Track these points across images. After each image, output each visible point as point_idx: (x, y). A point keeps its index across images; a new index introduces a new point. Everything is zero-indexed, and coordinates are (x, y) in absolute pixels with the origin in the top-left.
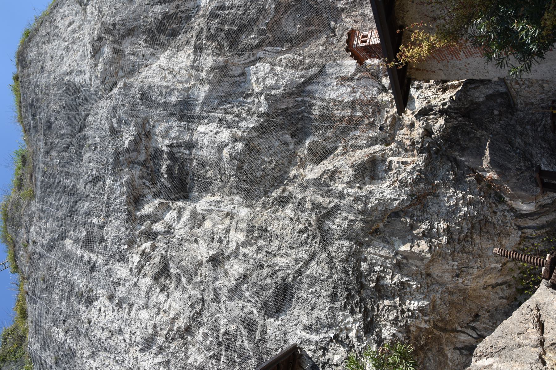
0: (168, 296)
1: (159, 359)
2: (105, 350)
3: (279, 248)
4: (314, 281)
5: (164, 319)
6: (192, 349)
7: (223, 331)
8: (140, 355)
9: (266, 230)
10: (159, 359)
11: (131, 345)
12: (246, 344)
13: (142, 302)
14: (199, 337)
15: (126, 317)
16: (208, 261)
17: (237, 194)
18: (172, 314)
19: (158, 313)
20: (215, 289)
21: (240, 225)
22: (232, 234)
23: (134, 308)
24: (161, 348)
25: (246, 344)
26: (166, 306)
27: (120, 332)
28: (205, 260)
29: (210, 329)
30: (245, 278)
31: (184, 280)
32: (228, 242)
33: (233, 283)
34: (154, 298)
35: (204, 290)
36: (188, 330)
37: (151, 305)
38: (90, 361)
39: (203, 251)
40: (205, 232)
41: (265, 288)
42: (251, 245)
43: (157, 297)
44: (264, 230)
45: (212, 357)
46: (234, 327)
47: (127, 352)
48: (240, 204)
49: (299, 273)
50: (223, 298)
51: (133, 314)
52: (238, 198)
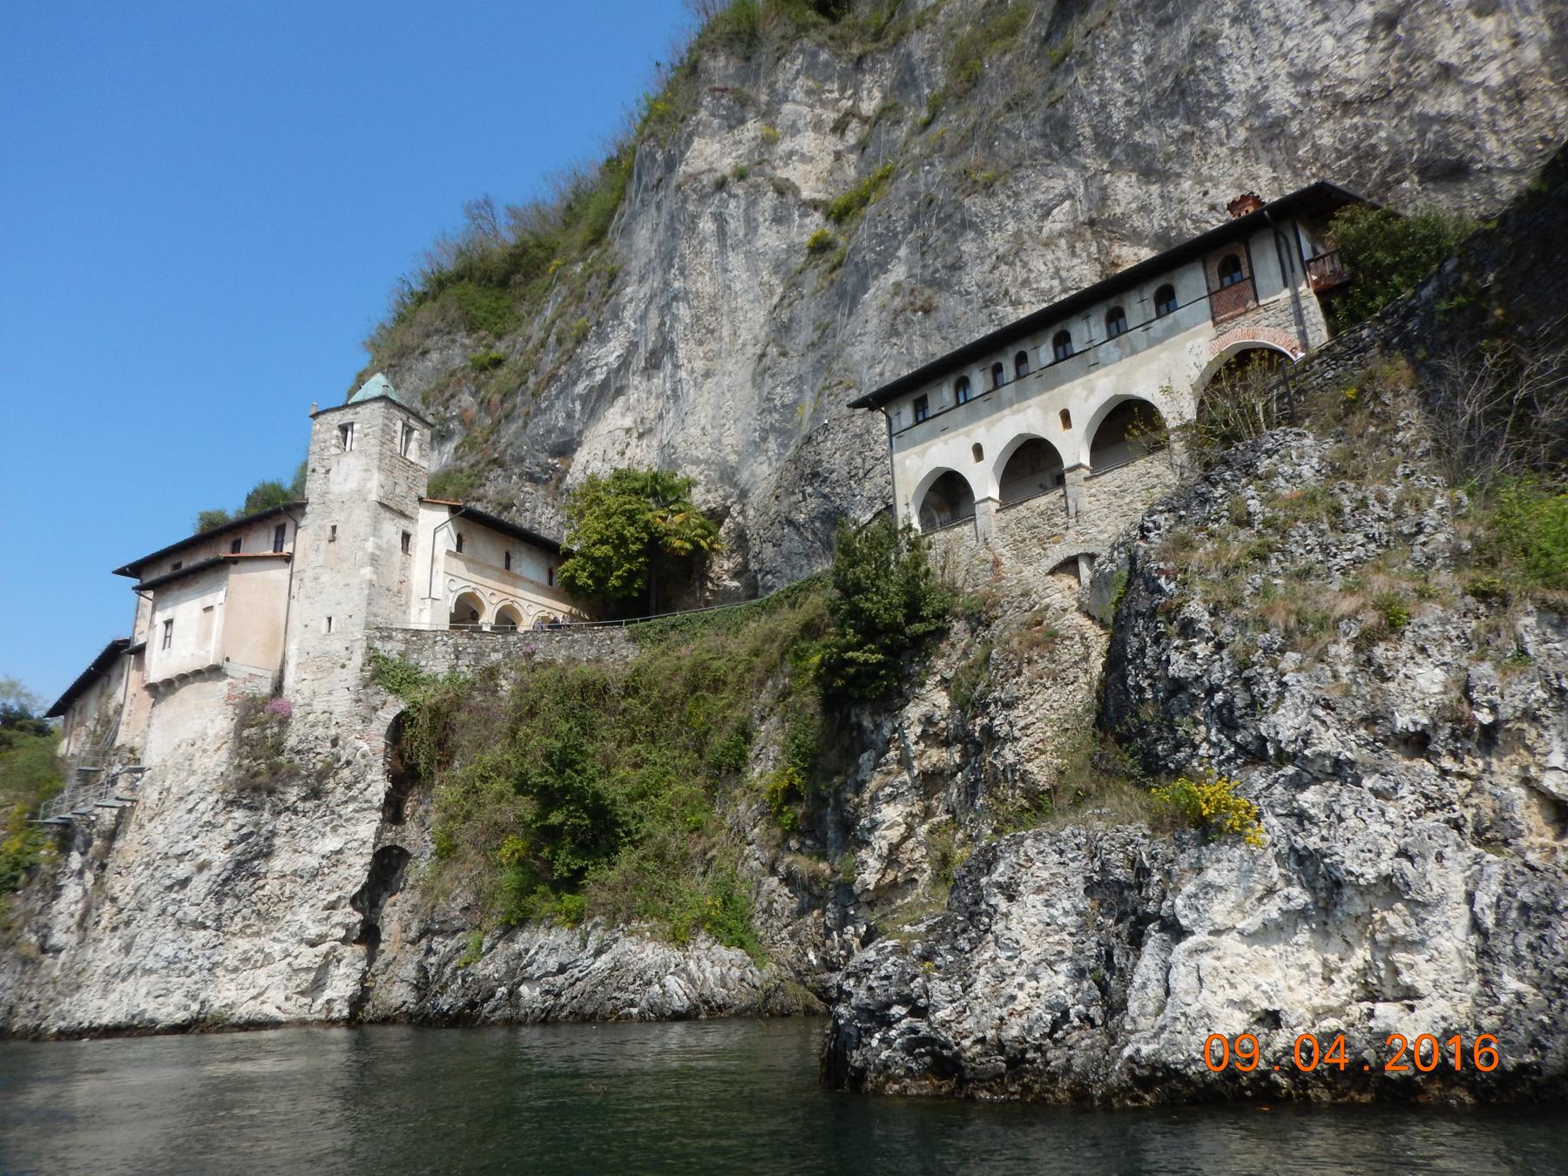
0: (1367, 51)
1: (1296, 101)
2: (1253, 30)
3: (1507, 131)
4: (1490, 191)
5: (1340, 71)
6: (1330, 124)
7: (1373, 141)
8: (1283, 77)
9: (1521, 101)
10: (1296, 101)
11: (1284, 56)
12: (1375, 174)
13: (1340, 29)
14: (1347, 122)
15: (1308, 23)
16: (1440, 64)
17: (1553, 28)
18: (1353, 74)
19: (1341, 58)
20: (1412, 95)
21: (1510, 66)
22: (1494, 65)
23: (1329, 25)
24: (1309, 93)
25: (1375, 174)
26: (1355, 60)
27: (1287, 31)
28: (1439, 58)
29: (1365, 126)
30: (1445, 119)
31: (1397, 51)
32: (1479, 69)
33: (1432, 112)
34: (1355, 37)
35: (1402, 86)
36: (1347, 105)
37: (1345, 42)
38: (1227, 21)
39: (1449, 49)
40: (1474, 32)
41: (1449, 150)
42: (1492, 98)
43: (1358, 41)
44: (1520, 97)
45: (1337, 150)
46: (1384, 149)
47: (1272, 58)
48: (1541, 42)
49: (1489, 170)
50: (1407, 114)
51: (1319, 29)
52: (1547, 33)
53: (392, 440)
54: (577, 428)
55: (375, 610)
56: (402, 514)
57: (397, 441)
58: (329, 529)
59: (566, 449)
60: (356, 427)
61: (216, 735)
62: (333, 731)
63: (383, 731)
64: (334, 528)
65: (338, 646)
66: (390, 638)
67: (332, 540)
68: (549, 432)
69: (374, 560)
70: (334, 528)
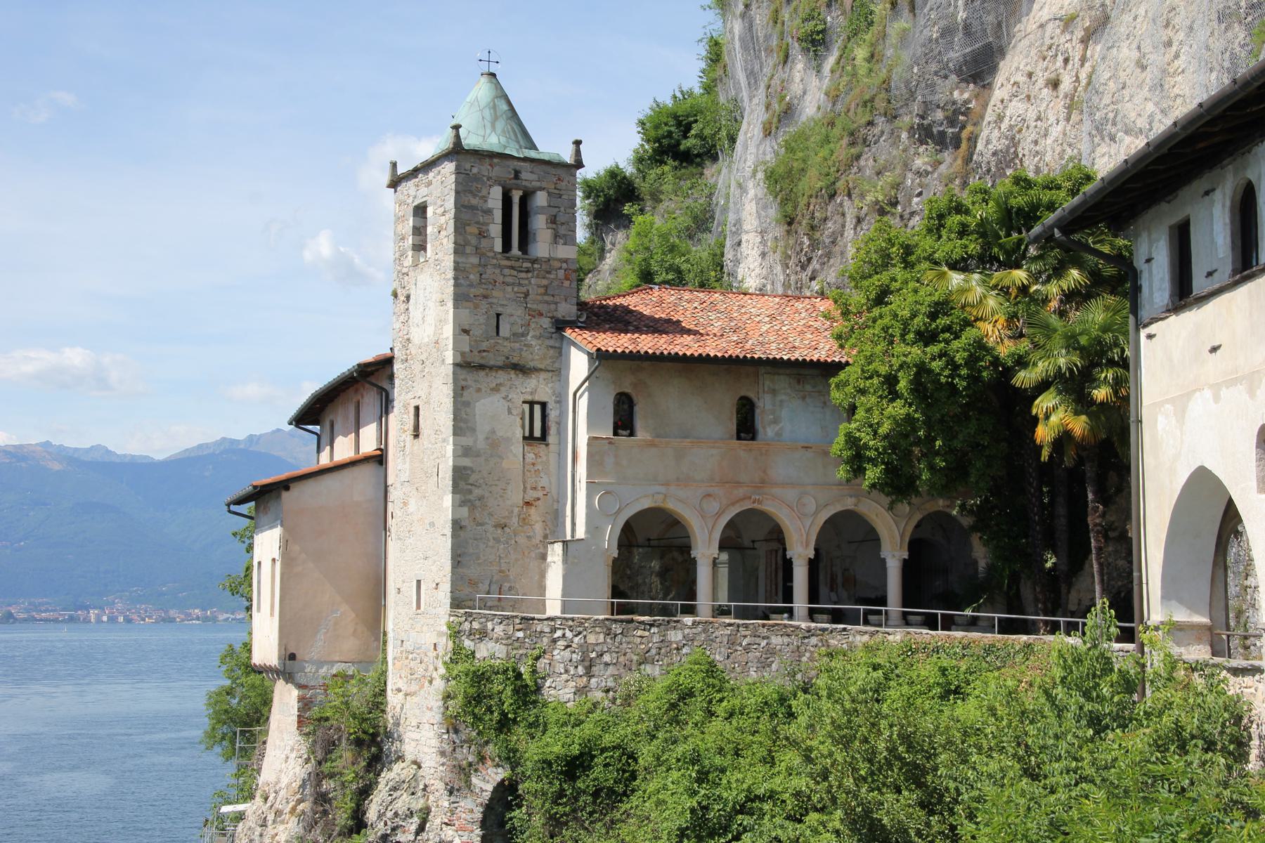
53: (482, 235)
54: (990, 19)
55: (472, 571)
56: (521, 369)
57: (496, 229)
58: (412, 411)
59: (980, 68)
60: (430, 211)
61: (288, 786)
62: (418, 804)
63: (478, 816)
64: (417, 408)
65: (428, 638)
66: (483, 634)
67: (416, 436)
68: (947, 32)
69: (462, 479)
70: (417, 408)
